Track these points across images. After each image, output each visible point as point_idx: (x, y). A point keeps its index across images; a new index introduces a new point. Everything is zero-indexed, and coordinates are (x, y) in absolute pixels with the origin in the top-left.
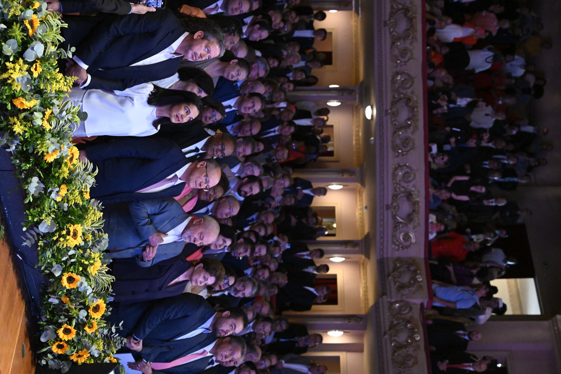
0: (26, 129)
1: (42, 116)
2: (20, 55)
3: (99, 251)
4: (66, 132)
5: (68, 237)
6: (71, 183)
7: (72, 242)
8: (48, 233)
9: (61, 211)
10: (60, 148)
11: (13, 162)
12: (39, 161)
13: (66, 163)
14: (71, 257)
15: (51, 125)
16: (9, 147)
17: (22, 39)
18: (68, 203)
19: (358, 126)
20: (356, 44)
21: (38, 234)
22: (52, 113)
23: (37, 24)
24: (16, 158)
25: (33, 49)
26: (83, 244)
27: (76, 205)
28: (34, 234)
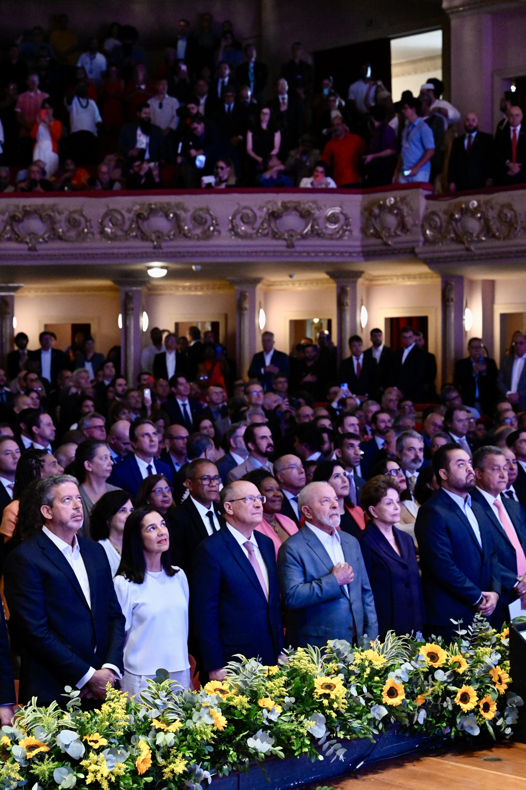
0: (181, 755)
1: (162, 733)
2: (75, 764)
3: (351, 652)
4: (185, 700)
5: (333, 697)
6: (255, 692)
7: (339, 691)
8: (326, 724)
9: (295, 706)
10: (207, 707)
11: (227, 774)
12: (224, 738)
13: (229, 699)
14: (360, 692)
15: (175, 720)
16: (206, 780)
17: (53, 761)
18: (284, 697)
19: (177, 287)
20: (61, 290)
21: (328, 738)
22: (157, 718)
23: (32, 740)
24: (221, 769)
25: (67, 746)
26: (341, 676)
27: (287, 685)
28: (327, 744)
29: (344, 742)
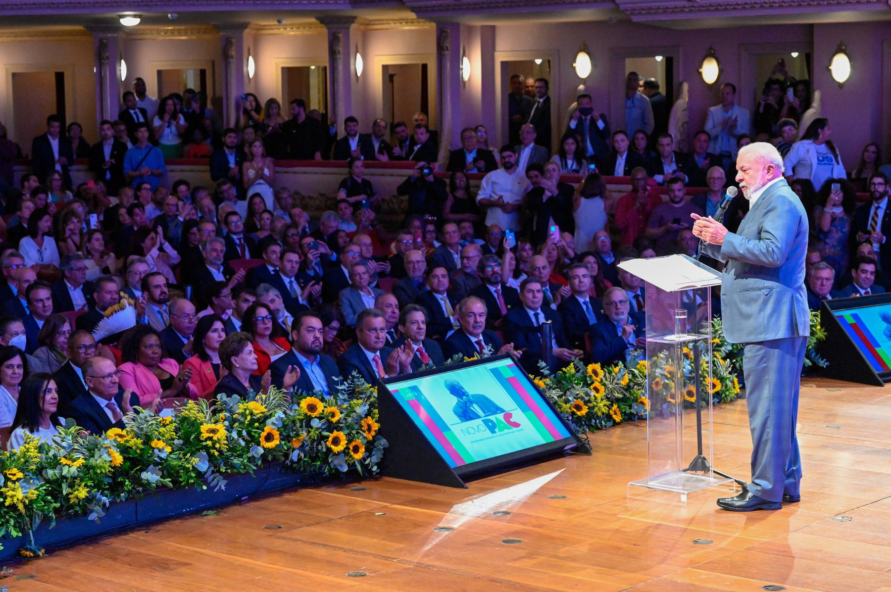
10: (106, 448)
11: (124, 500)
13: (127, 441)
16: (104, 504)
18: (173, 439)
22: (64, 457)
24: (119, 496)
27: (177, 430)
29: (225, 476)
